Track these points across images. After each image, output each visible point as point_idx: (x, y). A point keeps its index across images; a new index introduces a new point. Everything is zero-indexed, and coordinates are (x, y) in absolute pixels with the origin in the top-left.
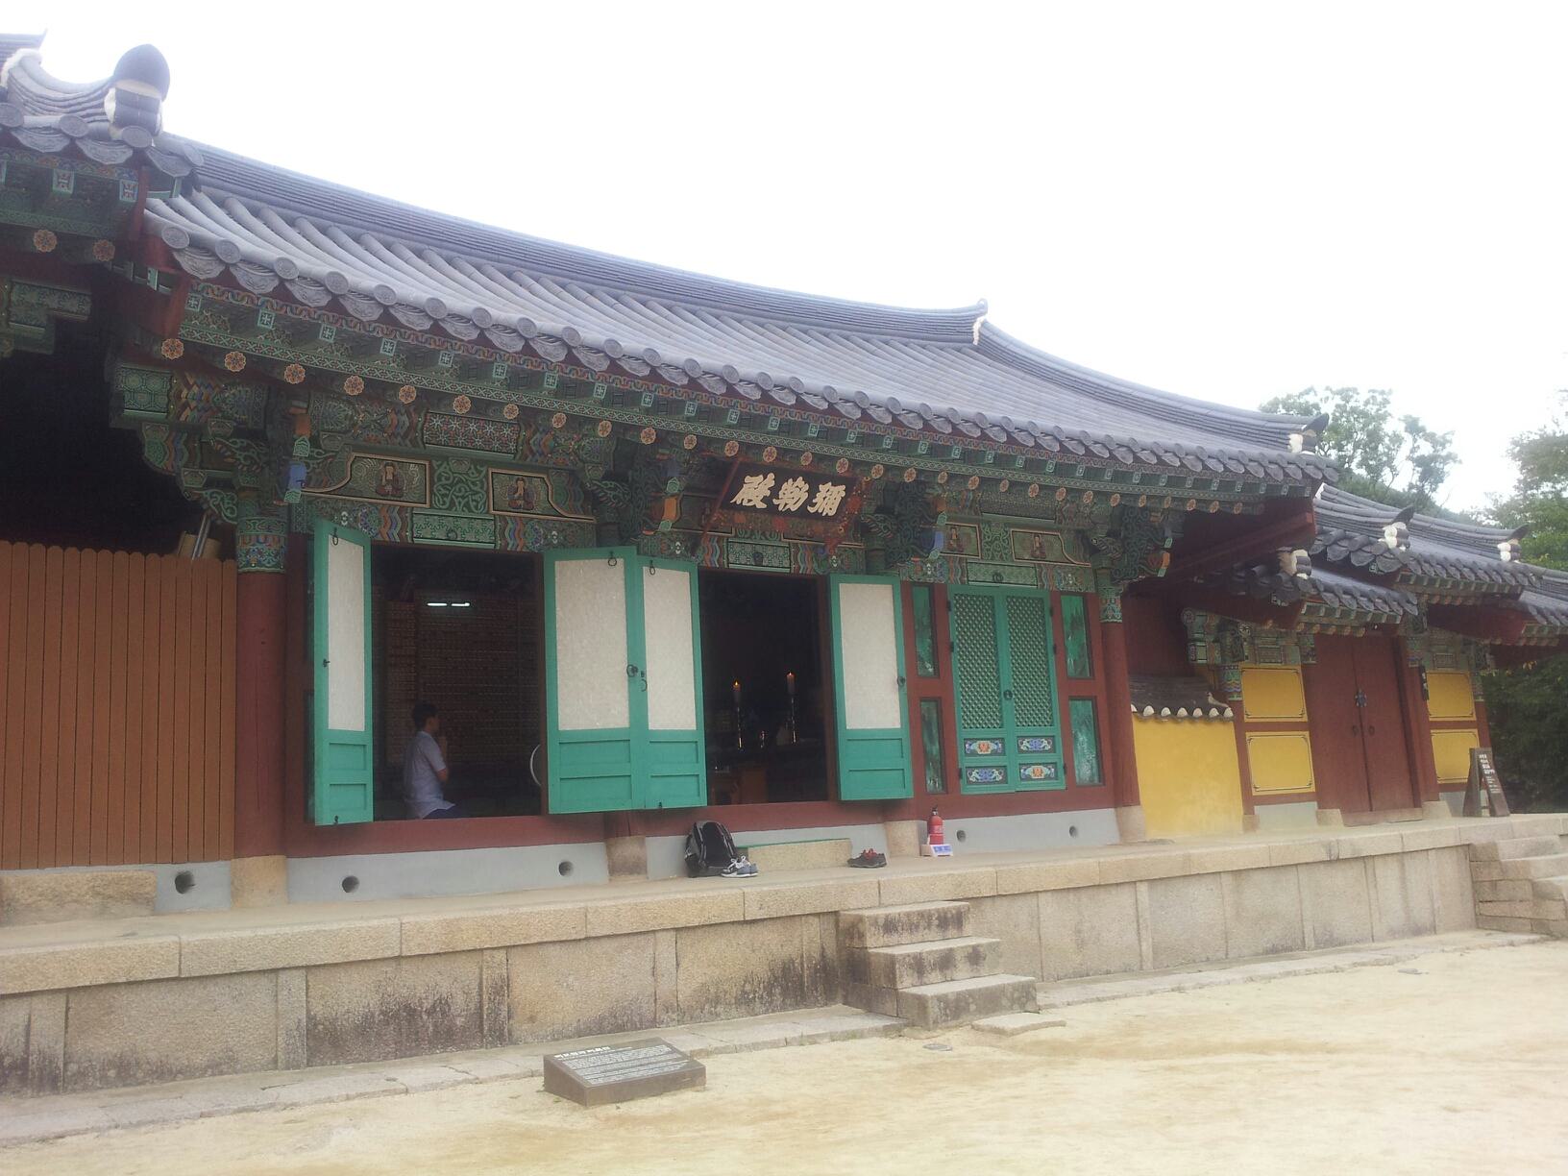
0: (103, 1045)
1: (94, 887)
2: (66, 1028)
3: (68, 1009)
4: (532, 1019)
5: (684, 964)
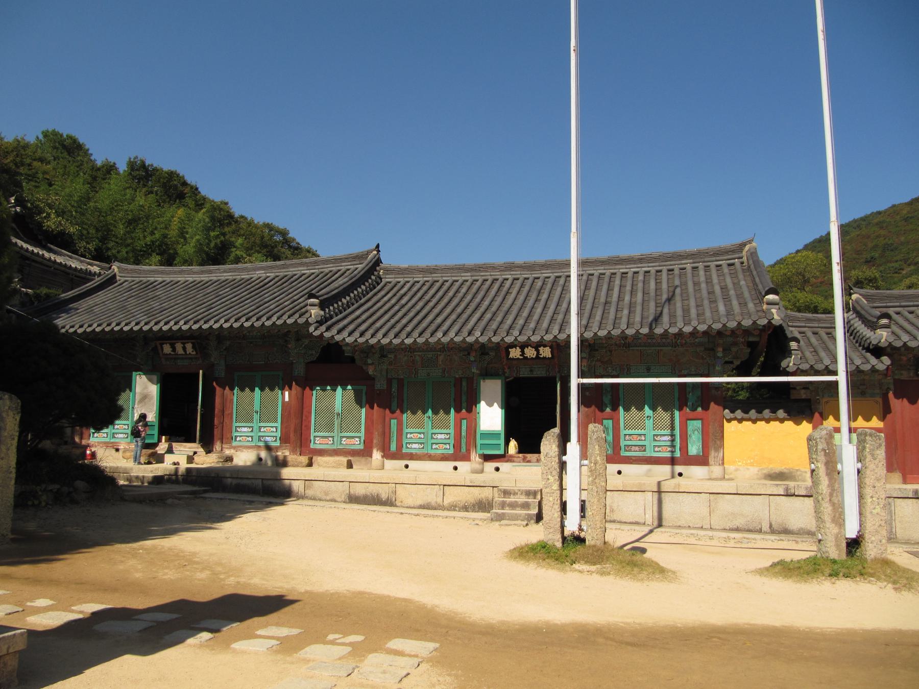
0: (309, 493)
4: (401, 502)
5: (446, 495)
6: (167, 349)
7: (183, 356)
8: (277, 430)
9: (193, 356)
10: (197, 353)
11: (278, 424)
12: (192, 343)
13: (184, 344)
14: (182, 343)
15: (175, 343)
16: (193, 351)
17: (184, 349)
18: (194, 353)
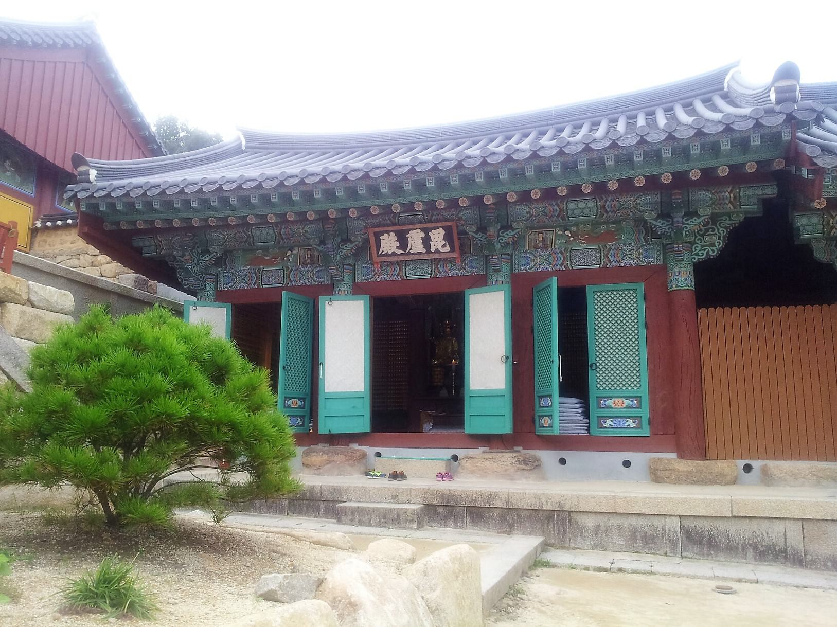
1: (812, 471)
2: (803, 537)
3: (803, 528)
6: (389, 244)
7: (422, 257)
8: (599, 403)
9: (443, 256)
10: (452, 250)
11: (644, 392)
12: (444, 228)
13: (426, 231)
14: (422, 230)
15: (407, 231)
16: (444, 246)
17: (426, 241)
18: (448, 249)
